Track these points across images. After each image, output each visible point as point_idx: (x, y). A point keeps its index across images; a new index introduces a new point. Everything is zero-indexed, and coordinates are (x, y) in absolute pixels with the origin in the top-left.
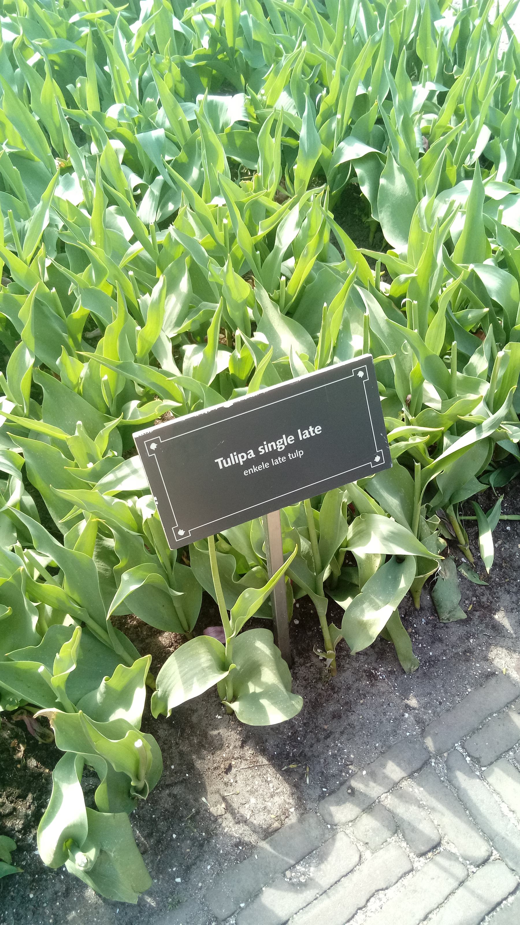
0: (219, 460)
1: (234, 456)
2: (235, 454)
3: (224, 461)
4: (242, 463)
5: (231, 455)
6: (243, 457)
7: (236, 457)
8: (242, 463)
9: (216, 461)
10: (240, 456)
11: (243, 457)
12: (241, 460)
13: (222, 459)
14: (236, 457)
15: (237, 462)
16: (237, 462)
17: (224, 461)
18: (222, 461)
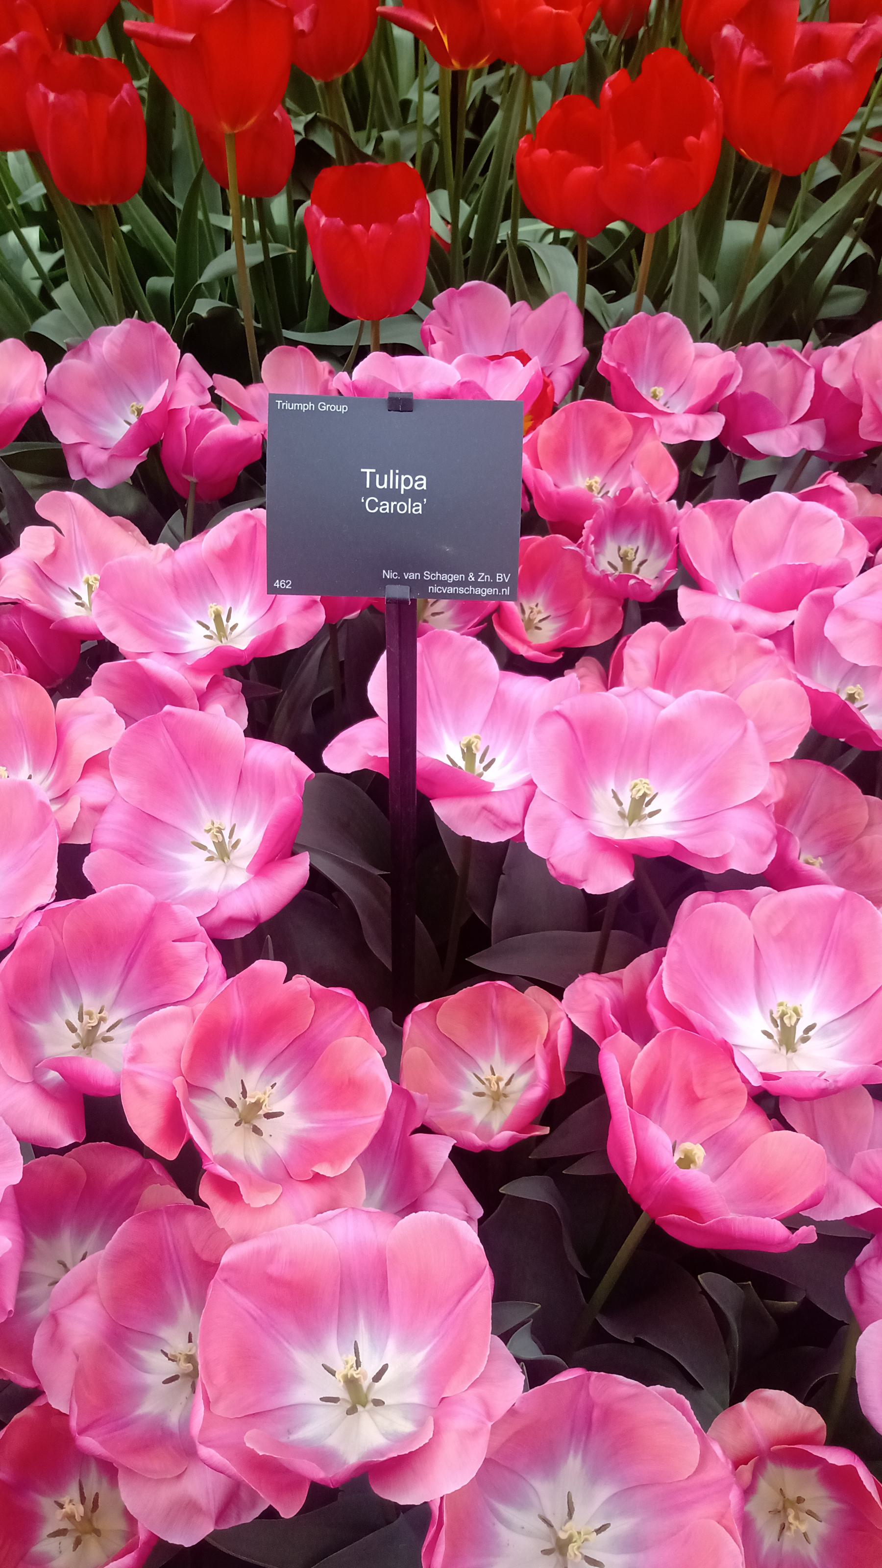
0: (368, 471)
1: (395, 474)
2: (397, 471)
3: (378, 476)
4: (402, 492)
5: (392, 471)
6: (407, 482)
7: (397, 477)
8: (402, 492)
9: (362, 470)
11: (407, 482)
12: (403, 487)
13: (374, 470)
14: (397, 477)
15: (397, 487)
16: (397, 487)
17: (378, 476)
18: (373, 475)
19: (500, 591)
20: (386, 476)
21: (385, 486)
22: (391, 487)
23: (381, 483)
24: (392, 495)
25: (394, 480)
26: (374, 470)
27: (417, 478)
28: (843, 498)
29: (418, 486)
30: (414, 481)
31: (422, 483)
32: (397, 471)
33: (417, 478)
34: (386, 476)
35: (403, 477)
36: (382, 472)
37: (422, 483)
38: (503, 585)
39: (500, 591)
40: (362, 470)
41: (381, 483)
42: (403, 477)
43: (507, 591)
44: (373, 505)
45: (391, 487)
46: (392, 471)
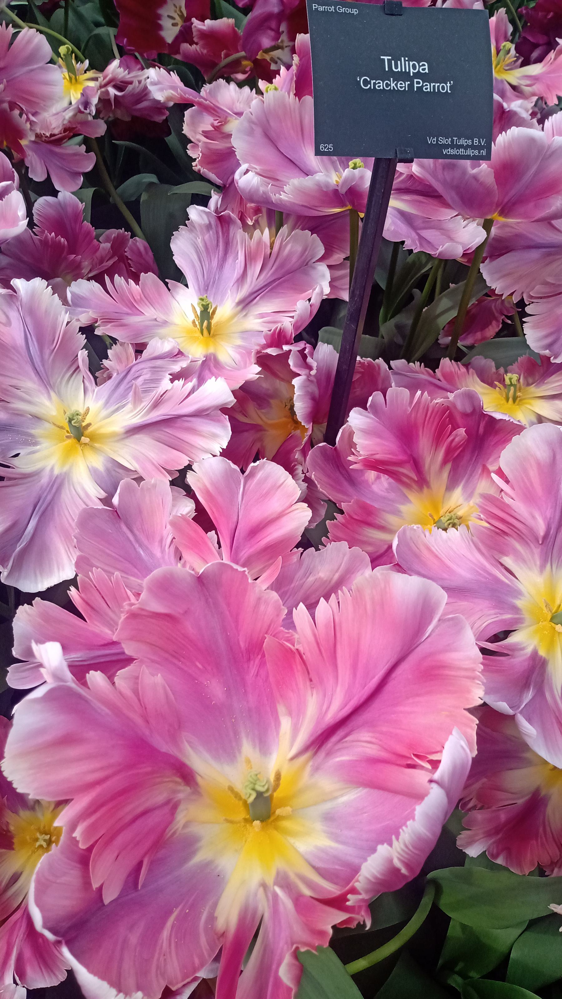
0: (386, 58)
1: (405, 61)
2: (407, 59)
3: (393, 62)
4: (412, 75)
5: (403, 58)
6: (414, 67)
7: (407, 62)
8: (412, 75)
9: (382, 57)
10: (411, 63)
11: (414, 67)
12: (412, 70)
13: (390, 58)
14: (407, 62)
15: (407, 71)
16: (407, 71)
17: (393, 62)
19: (479, 153)
20: (399, 62)
21: (399, 69)
22: (403, 70)
23: (396, 67)
24: (403, 76)
25: (405, 65)
26: (390, 58)
27: (421, 64)
28: (116, 34)
29: (424, 69)
30: (420, 66)
31: (424, 68)
32: (407, 59)
33: (421, 64)
34: (399, 62)
36: (396, 59)
38: (479, 148)
39: (479, 153)
40: (382, 57)
41: (396, 67)
42: (411, 63)
43: (484, 152)
44: (366, 83)
45: (403, 70)
46: (403, 58)
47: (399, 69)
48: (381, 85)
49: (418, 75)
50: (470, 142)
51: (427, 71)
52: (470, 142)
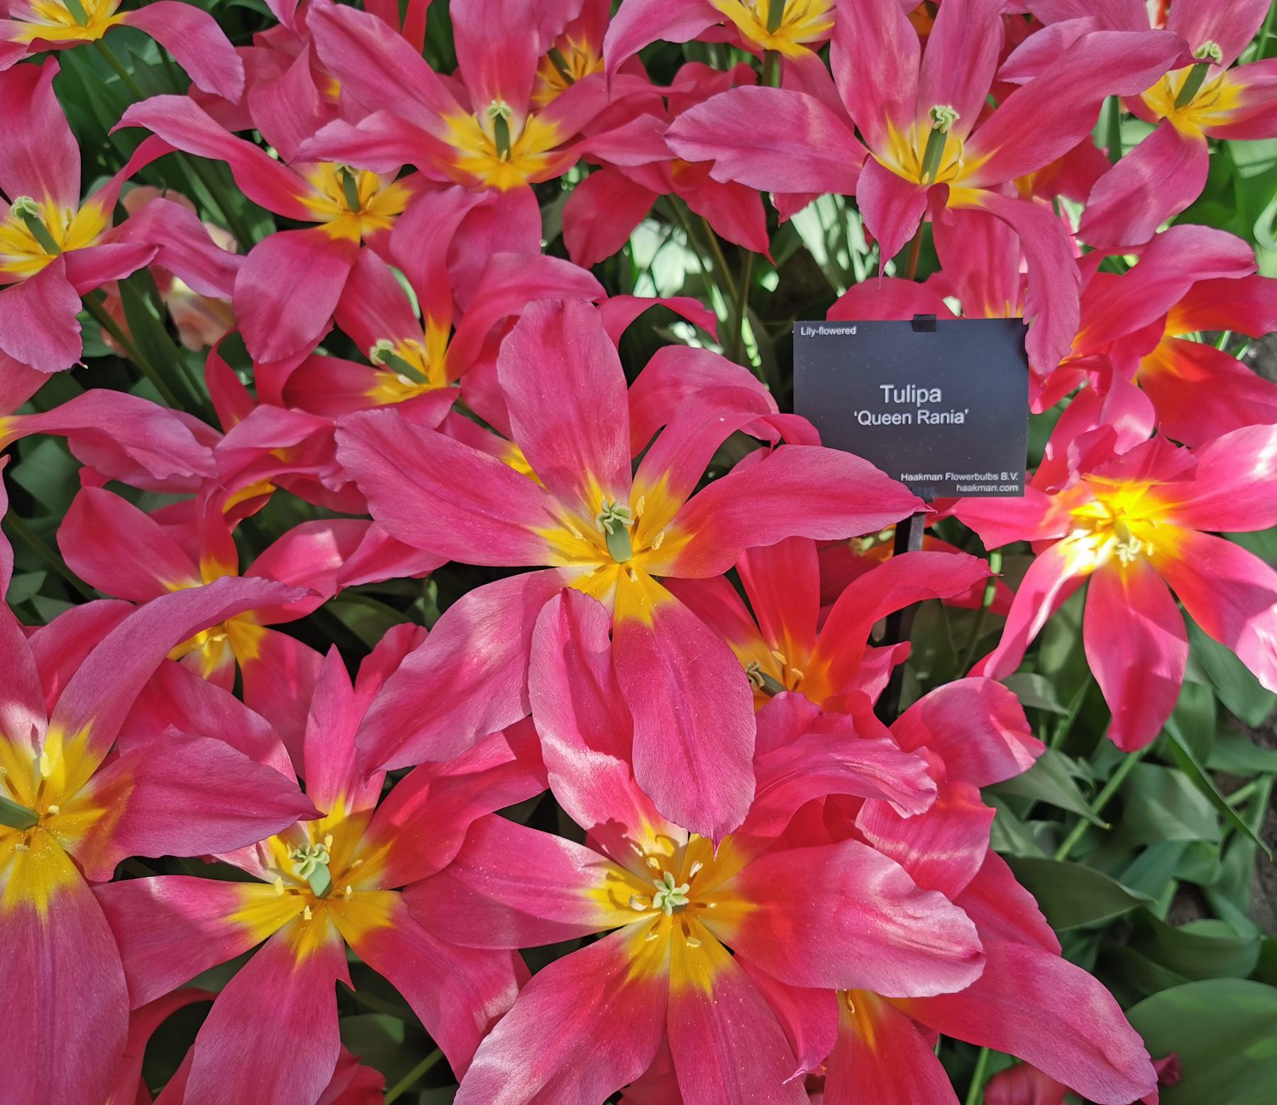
0: (887, 387)
3: (895, 392)
6: (923, 395)
10: (919, 392)
11: (923, 395)
12: (919, 400)
17: (895, 392)
18: (891, 391)
23: (899, 397)
35: (919, 392)
36: (900, 387)
37: (937, 395)
41: (899, 397)
43: (1015, 488)
47: (903, 400)
48: (885, 419)
49: (926, 405)
50: (996, 477)
51: (939, 400)
52: (996, 477)
